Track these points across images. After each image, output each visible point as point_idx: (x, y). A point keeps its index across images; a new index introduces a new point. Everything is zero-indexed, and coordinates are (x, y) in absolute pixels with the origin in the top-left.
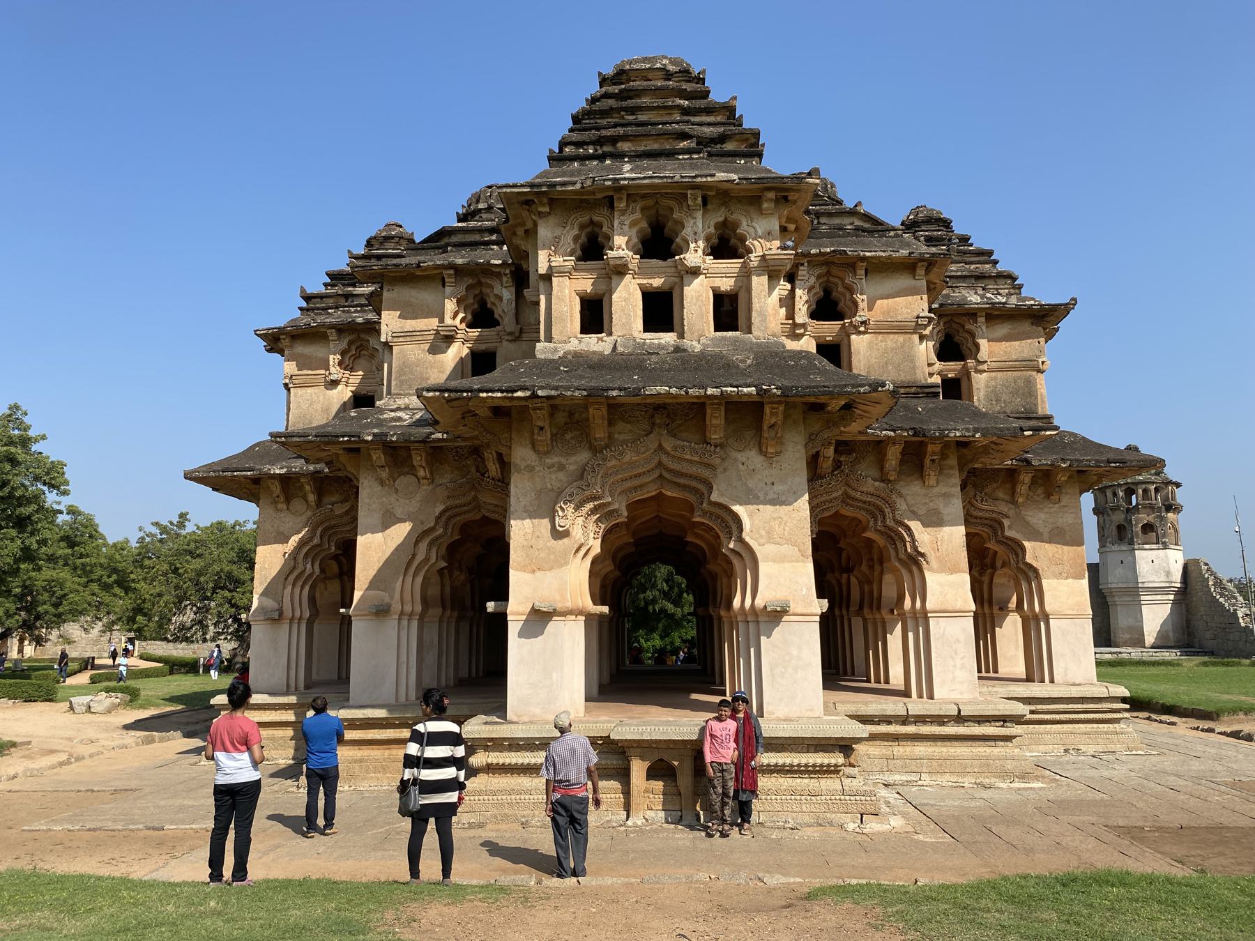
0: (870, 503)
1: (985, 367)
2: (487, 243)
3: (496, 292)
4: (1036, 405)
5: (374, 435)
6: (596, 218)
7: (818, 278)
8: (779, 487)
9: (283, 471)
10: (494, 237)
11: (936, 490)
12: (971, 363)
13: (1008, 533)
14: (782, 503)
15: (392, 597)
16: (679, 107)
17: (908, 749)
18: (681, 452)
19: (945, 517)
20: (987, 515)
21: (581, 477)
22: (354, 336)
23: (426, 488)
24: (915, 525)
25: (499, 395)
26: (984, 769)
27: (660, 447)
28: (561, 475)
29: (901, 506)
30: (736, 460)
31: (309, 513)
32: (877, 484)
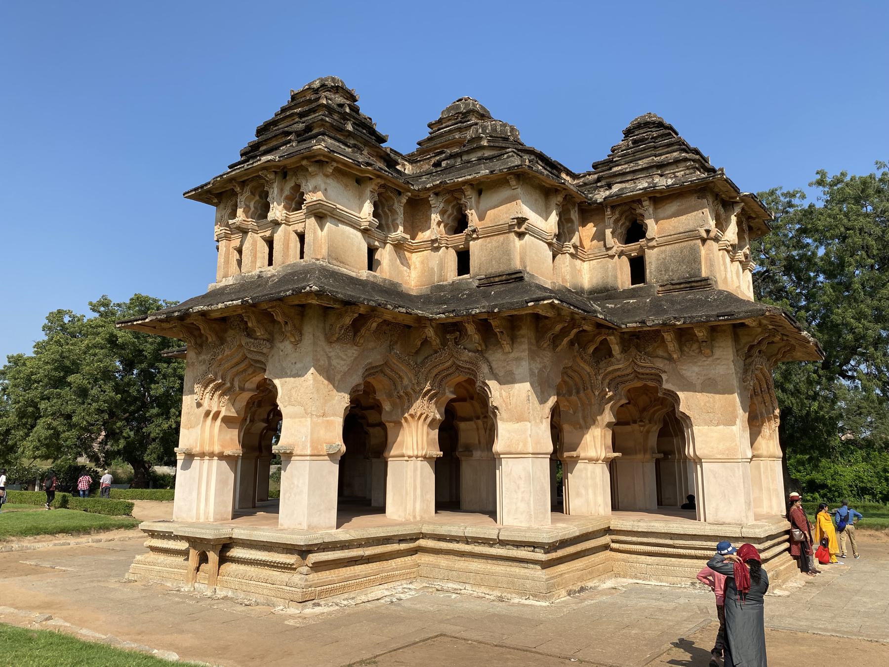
0: (469, 369)
1: (654, 243)
4: (700, 270)
7: (447, 202)
8: (299, 365)
11: (512, 355)
12: (642, 242)
13: (666, 386)
14: (299, 376)
16: (296, 114)
17: (466, 564)
19: (517, 377)
20: (648, 371)
24: (492, 384)
26: (510, 586)
27: (241, 346)
29: (485, 369)
30: (279, 348)
32: (470, 354)
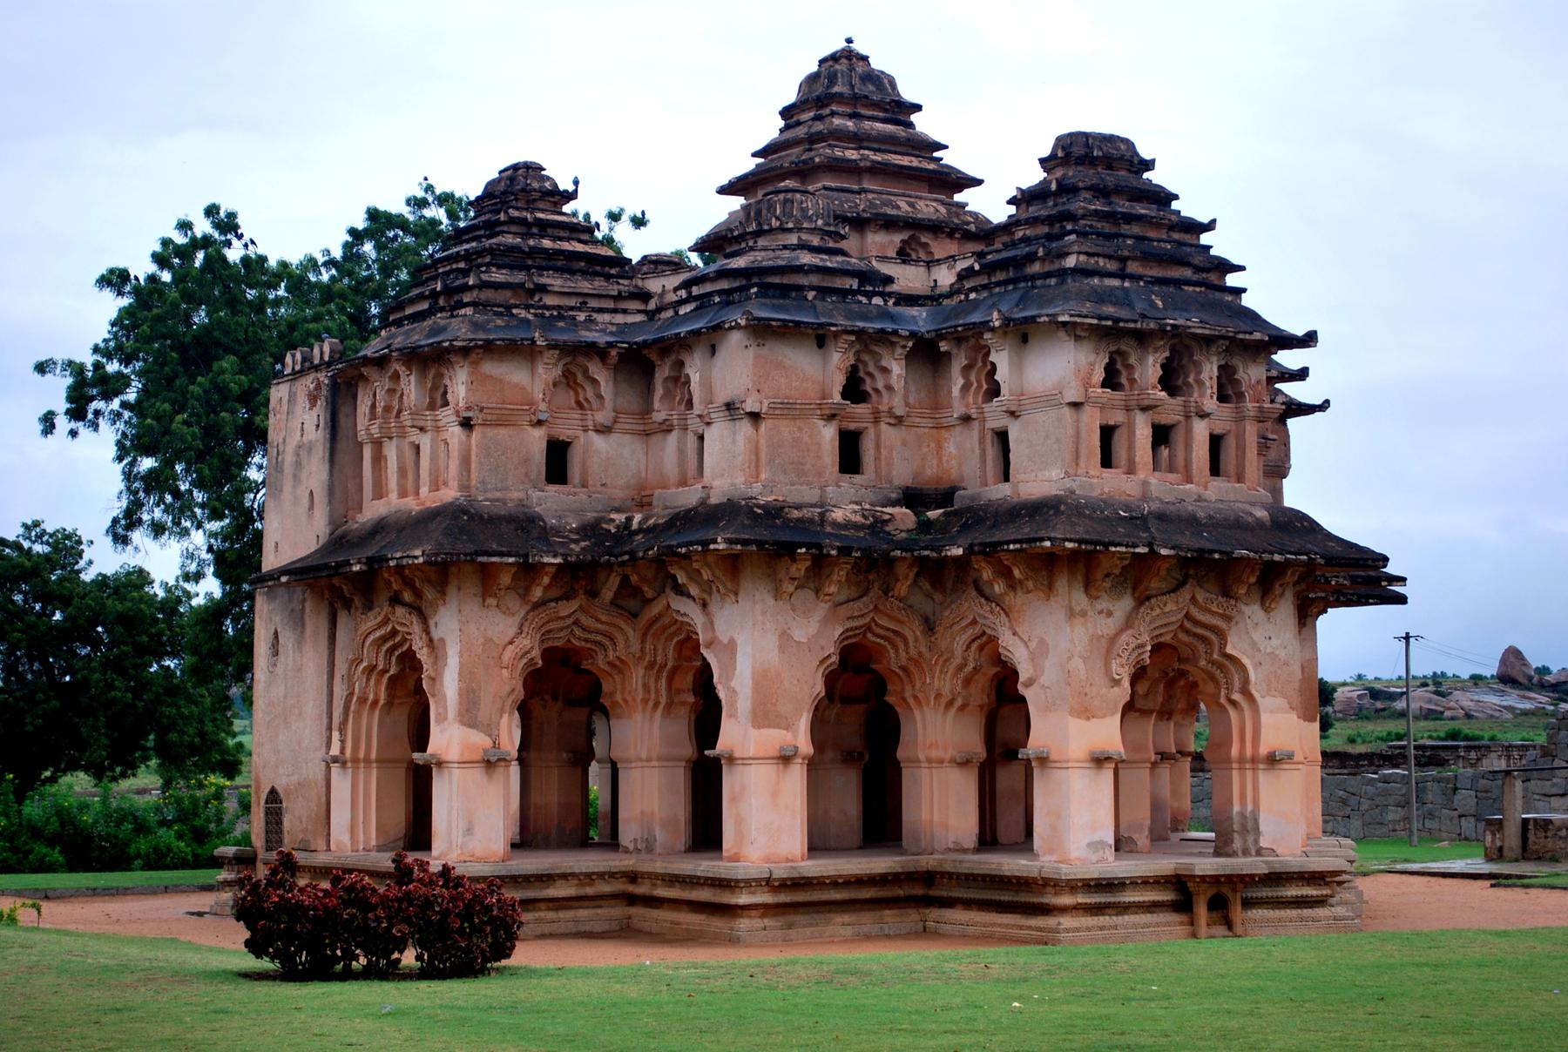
2: (854, 293)
3: (884, 363)
5: (840, 549)
6: (1124, 348)
9: (558, 560)
10: (854, 284)
15: (795, 737)
18: (1200, 601)
21: (1128, 624)
22: (568, 359)
23: (823, 608)
25: (1123, 549)
27: (1193, 600)
28: (1110, 620)
31: (523, 612)
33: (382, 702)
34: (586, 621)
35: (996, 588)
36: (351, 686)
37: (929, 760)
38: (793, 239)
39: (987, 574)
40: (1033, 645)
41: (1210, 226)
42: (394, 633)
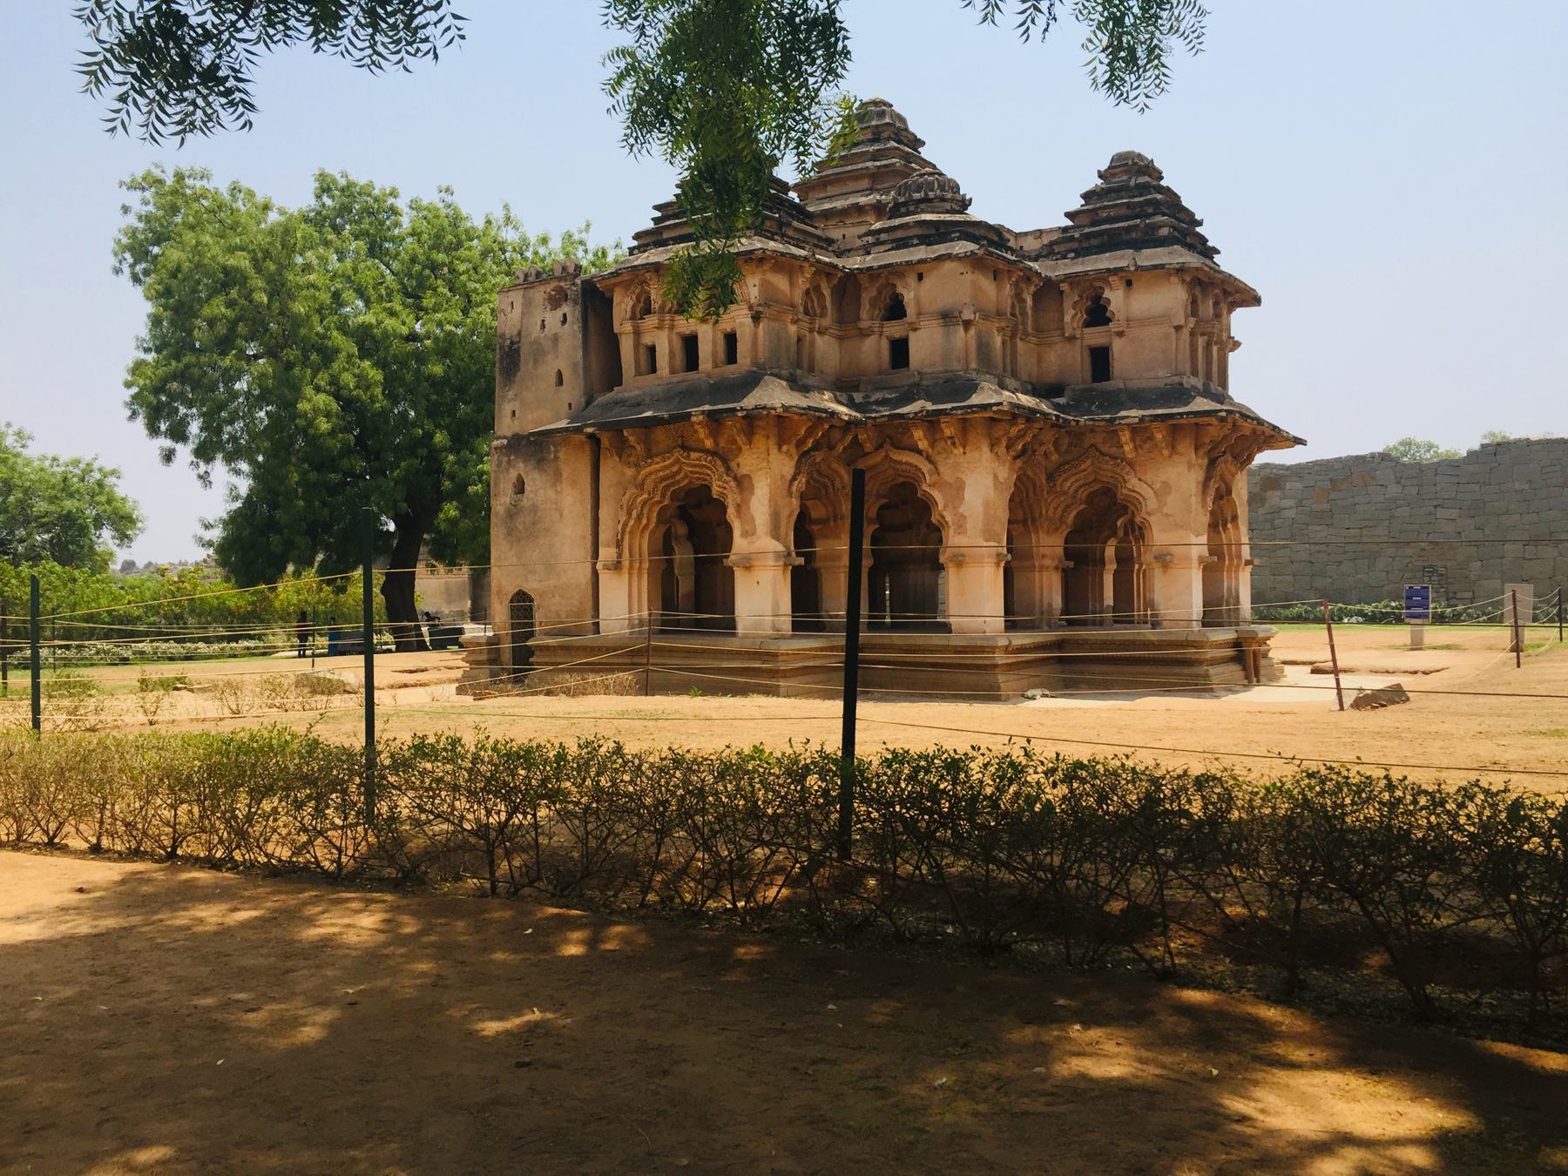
33: (652, 526)
34: (824, 467)
35: (1127, 448)
36: (629, 514)
37: (1042, 568)
38: (948, 206)
39: (1125, 437)
40: (1157, 486)
41: (1200, 223)
42: (677, 473)
